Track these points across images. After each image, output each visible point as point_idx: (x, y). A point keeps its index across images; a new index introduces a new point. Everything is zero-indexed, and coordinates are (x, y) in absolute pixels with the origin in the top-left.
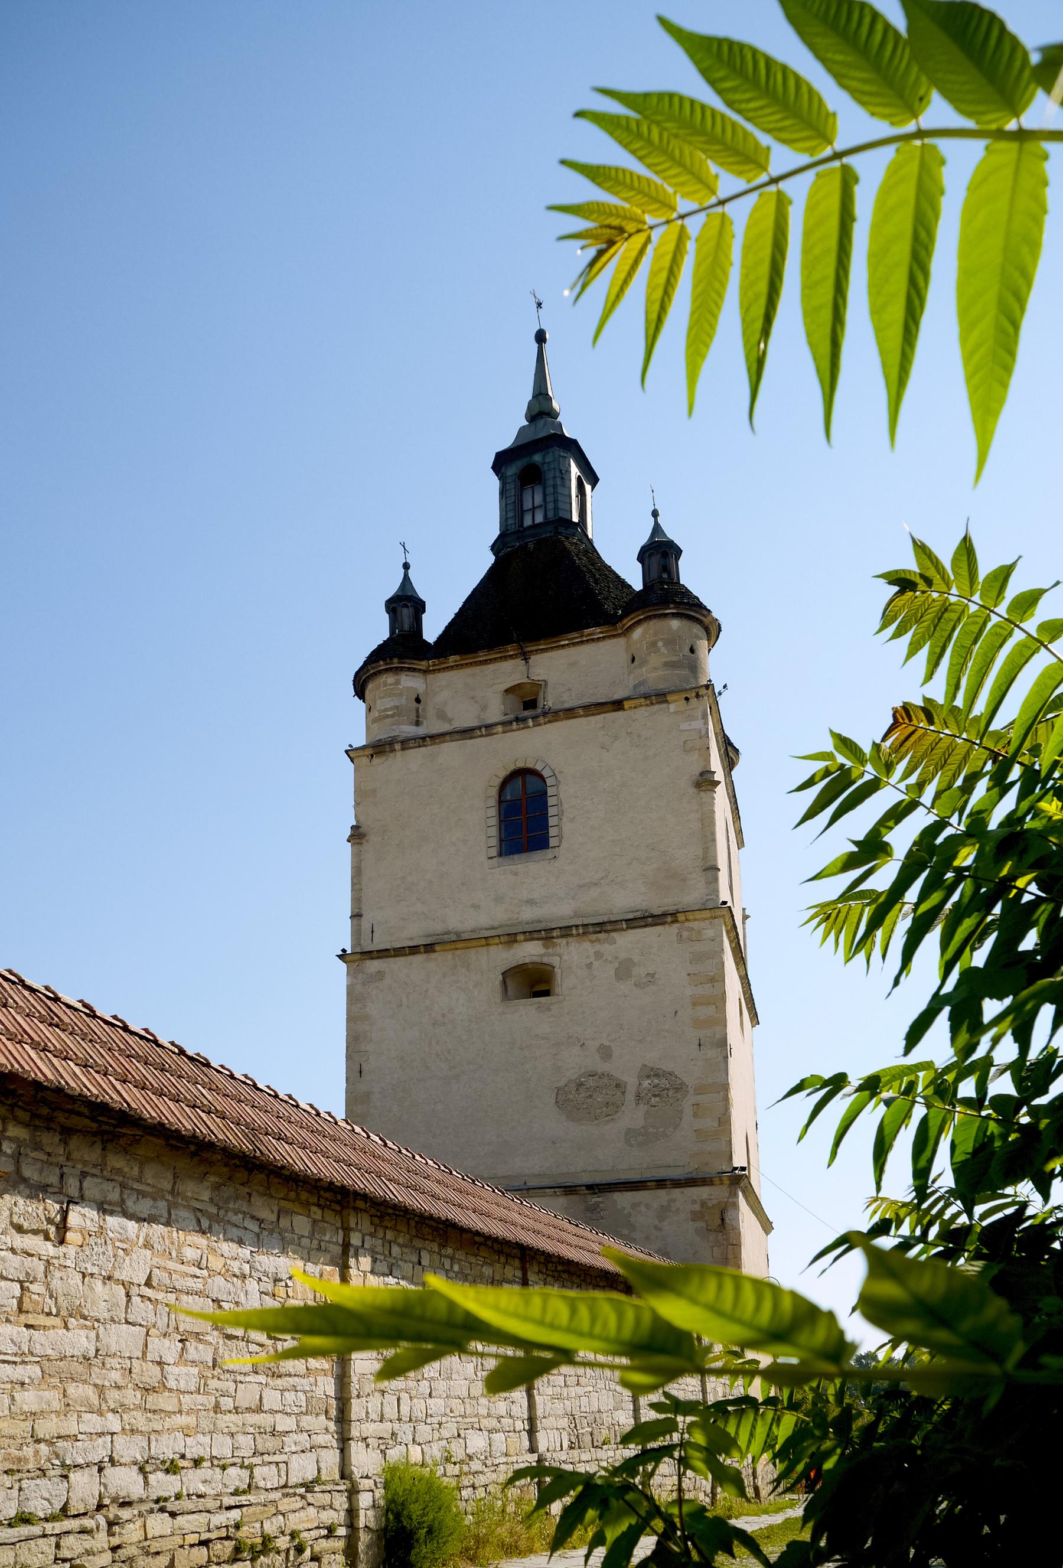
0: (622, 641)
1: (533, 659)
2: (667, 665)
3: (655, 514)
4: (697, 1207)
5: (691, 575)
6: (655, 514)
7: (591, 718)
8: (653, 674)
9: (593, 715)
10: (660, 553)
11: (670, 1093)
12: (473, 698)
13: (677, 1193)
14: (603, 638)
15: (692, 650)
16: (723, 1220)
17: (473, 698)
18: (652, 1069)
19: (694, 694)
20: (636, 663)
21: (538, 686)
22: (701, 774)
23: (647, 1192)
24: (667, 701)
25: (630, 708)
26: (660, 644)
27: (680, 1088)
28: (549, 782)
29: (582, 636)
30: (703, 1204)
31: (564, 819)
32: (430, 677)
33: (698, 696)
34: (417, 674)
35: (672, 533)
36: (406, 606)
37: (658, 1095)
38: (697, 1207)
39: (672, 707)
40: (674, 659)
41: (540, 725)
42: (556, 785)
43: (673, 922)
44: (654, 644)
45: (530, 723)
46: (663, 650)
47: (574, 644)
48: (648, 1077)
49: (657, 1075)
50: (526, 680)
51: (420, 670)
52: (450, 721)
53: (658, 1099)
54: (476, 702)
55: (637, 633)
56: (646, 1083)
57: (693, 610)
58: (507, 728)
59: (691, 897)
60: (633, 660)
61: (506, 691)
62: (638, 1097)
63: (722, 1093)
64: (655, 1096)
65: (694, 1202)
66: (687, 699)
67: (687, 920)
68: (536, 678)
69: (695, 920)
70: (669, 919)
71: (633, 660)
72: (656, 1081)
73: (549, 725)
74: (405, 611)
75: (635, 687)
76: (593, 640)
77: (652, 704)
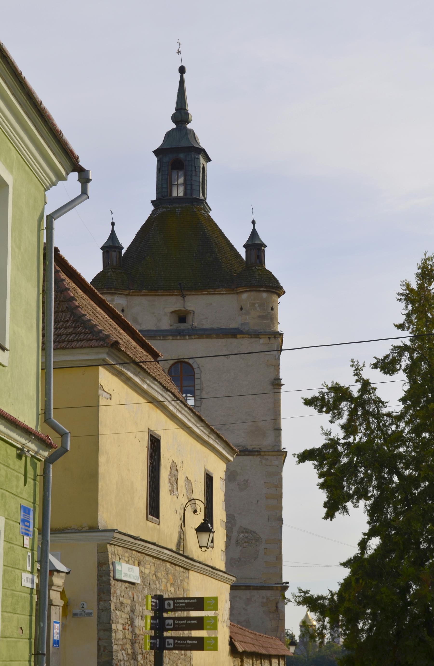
0: (235, 296)
1: (187, 298)
2: (260, 317)
3: (253, 222)
4: (265, 600)
5: (272, 263)
6: (253, 222)
7: (220, 340)
8: (251, 320)
9: (220, 338)
10: (255, 246)
11: (253, 542)
12: (153, 313)
13: (255, 592)
14: (226, 293)
15: (272, 309)
16: (277, 607)
17: (153, 313)
18: (245, 529)
19: (273, 336)
20: (243, 311)
21: (188, 312)
22: (275, 379)
23: (241, 591)
24: (259, 338)
25: (240, 338)
26: (257, 305)
27: (258, 540)
28: (196, 371)
29: (215, 291)
30: (268, 599)
31: (204, 392)
32: (129, 297)
33: (275, 337)
34: (123, 296)
35: (263, 237)
36: (114, 251)
37: (247, 542)
38: (265, 600)
39: (262, 341)
40: (263, 314)
41: (192, 339)
42: (201, 372)
43: (258, 455)
44: (253, 304)
45: (187, 337)
46: (258, 309)
47: (210, 294)
48: (242, 532)
49: (247, 532)
50: (183, 309)
51: (124, 294)
52: (140, 324)
53: (247, 544)
54: (155, 316)
55: (245, 296)
56: (241, 535)
57: (274, 288)
58: (175, 338)
59: (267, 442)
60: (241, 309)
61: (172, 312)
62: (237, 542)
63: (279, 544)
64: (245, 542)
65: (263, 598)
66: (269, 338)
67: (265, 455)
68: (189, 309)
69: (269, 455)
70: (256, 454)
71: (241, 309)
72: (246, 535)
73: (197, 340)
74: (114, 254)
75: (242, 324)
76: (220, 294)
77: (251, 338)
